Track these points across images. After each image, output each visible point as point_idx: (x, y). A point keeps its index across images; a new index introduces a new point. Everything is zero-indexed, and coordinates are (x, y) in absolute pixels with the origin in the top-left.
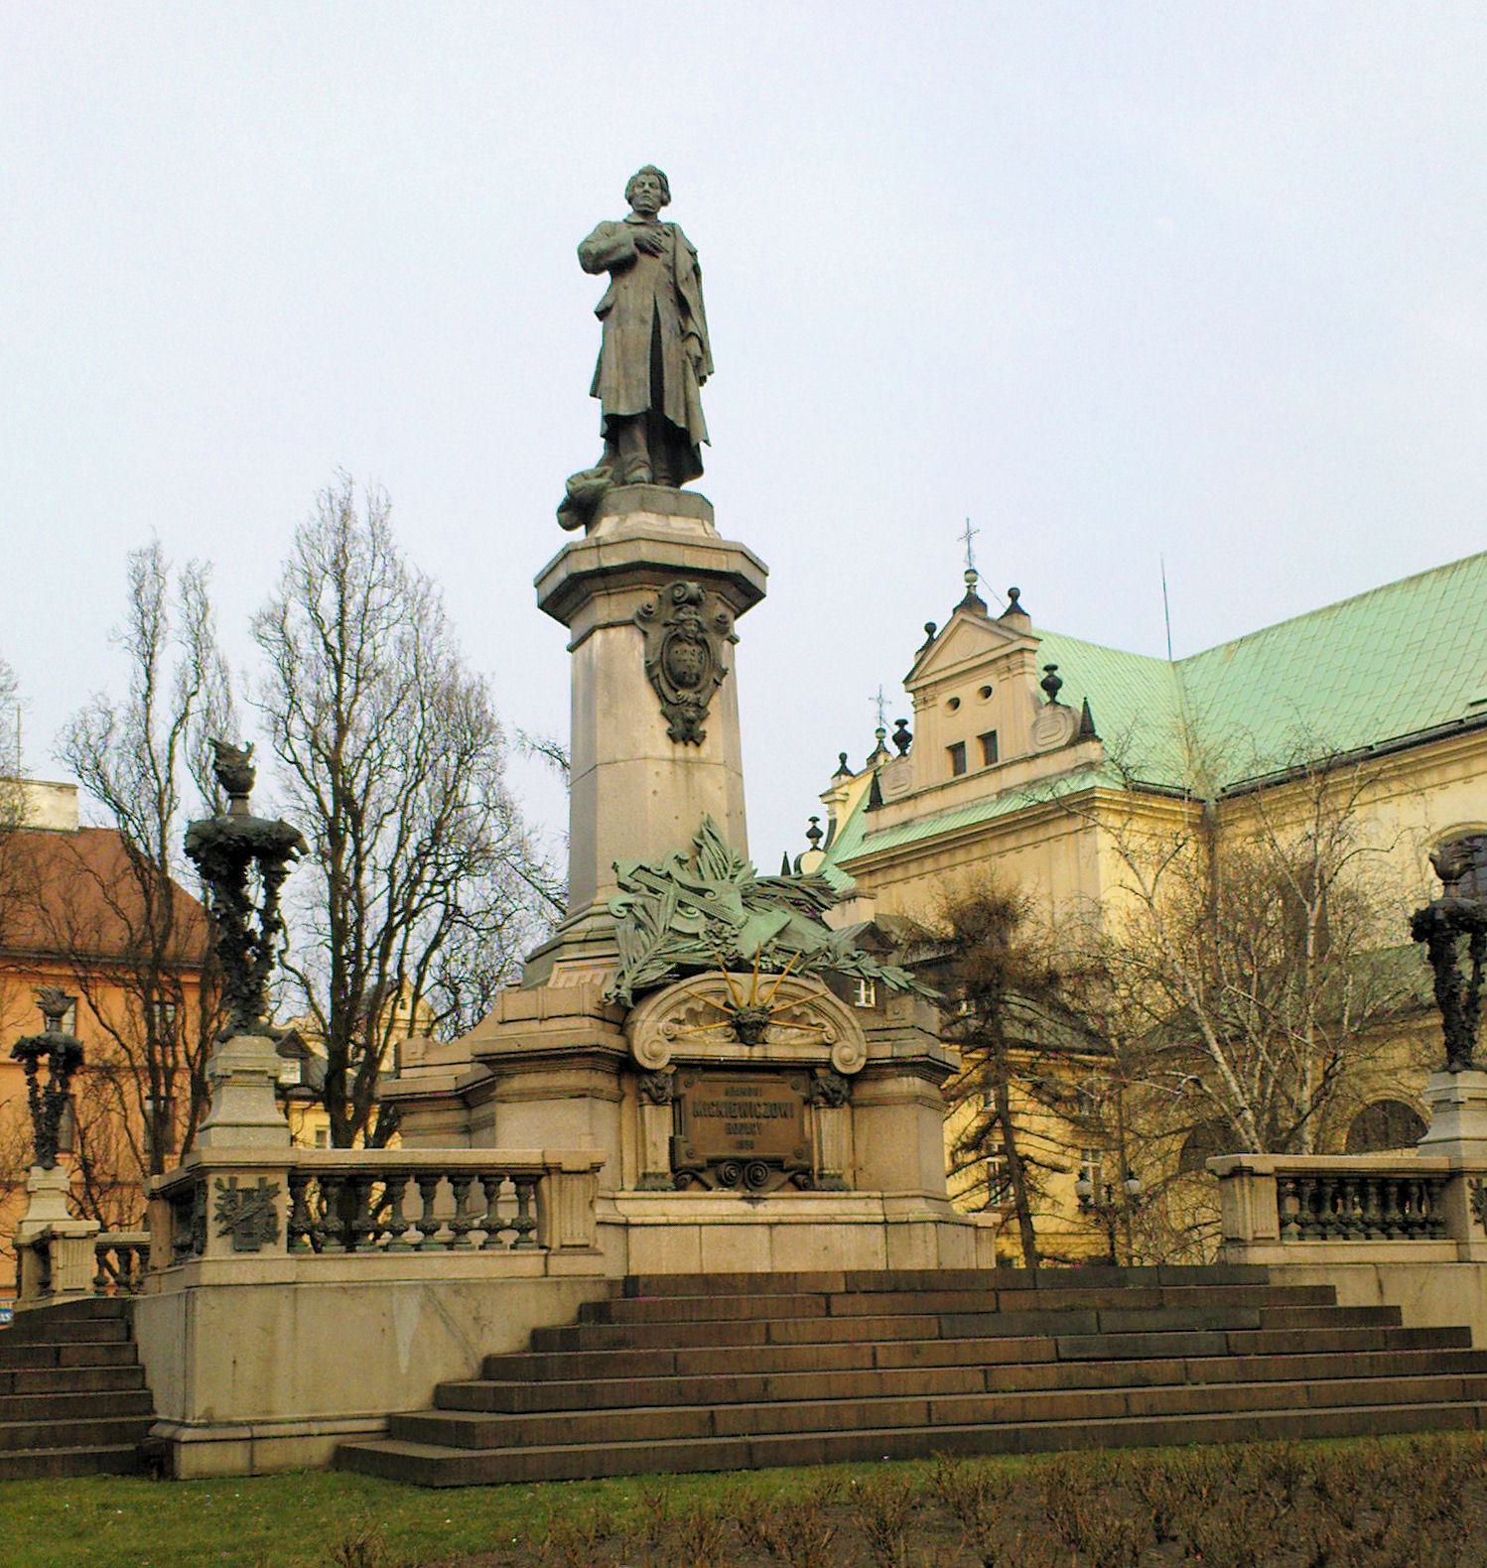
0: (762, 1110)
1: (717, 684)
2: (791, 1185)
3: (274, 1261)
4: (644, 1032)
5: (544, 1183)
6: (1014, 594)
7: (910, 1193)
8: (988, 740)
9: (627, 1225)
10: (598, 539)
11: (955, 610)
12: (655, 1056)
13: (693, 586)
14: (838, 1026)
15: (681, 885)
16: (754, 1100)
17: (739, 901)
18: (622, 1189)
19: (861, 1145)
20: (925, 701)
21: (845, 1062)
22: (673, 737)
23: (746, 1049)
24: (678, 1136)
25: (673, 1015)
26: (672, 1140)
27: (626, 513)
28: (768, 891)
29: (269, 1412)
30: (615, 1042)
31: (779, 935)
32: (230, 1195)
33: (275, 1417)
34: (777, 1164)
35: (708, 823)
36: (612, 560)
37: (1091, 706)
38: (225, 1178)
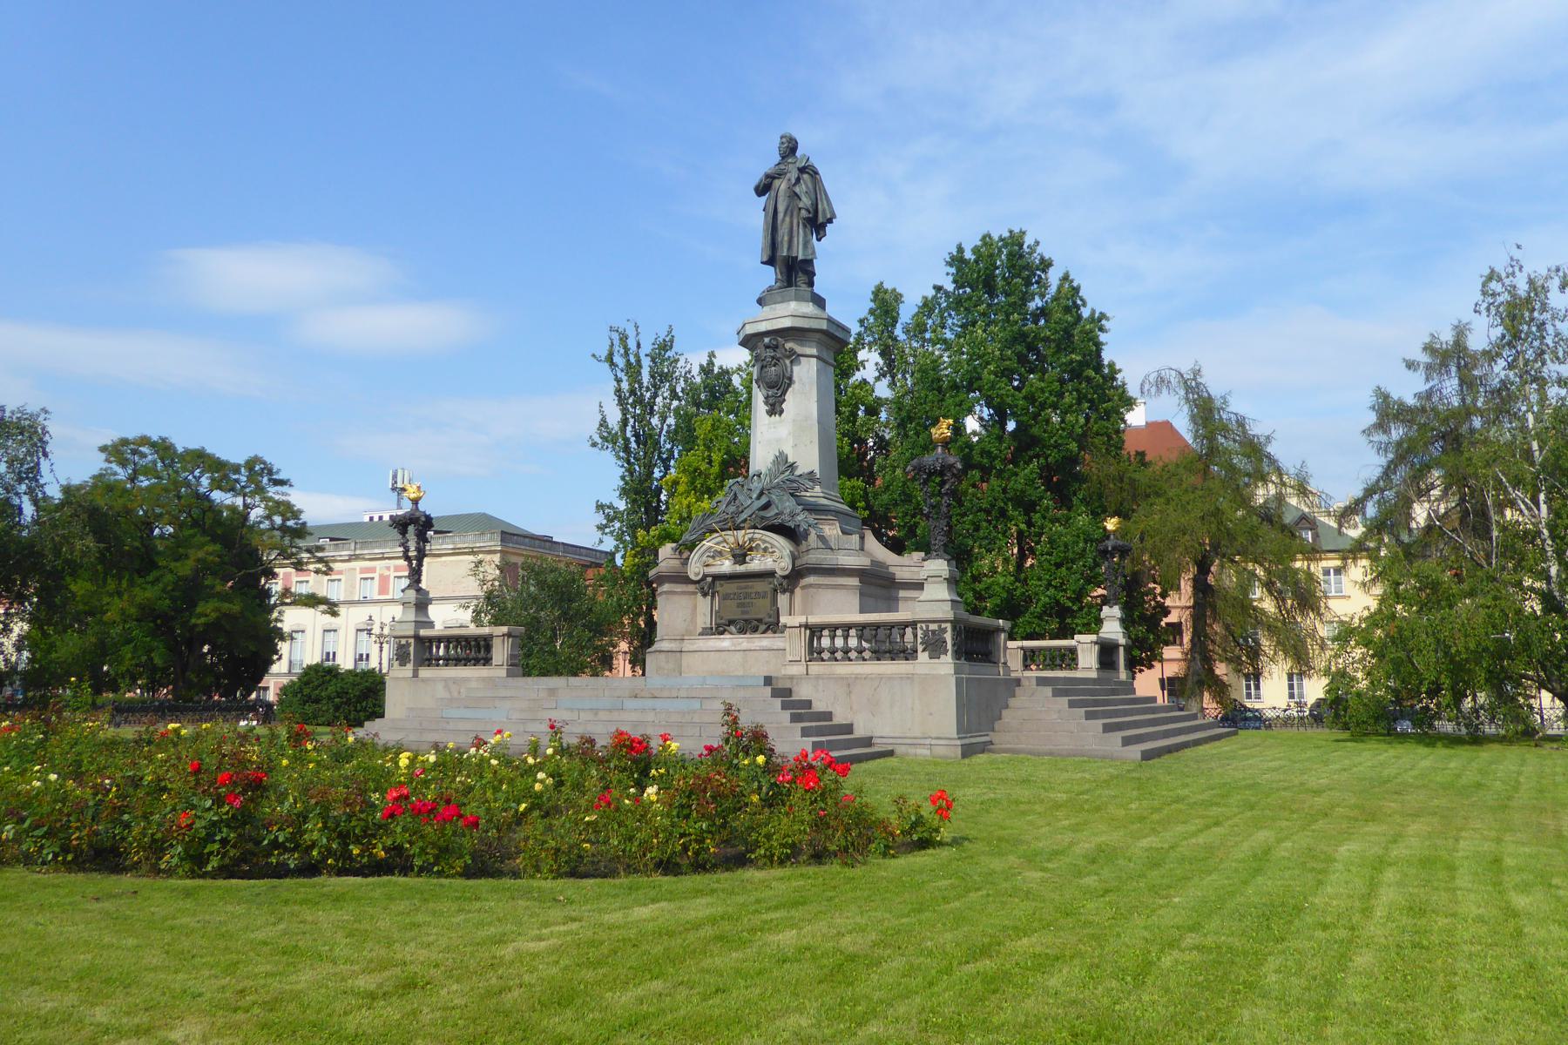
13: (767, 340)
34: (760, 621)
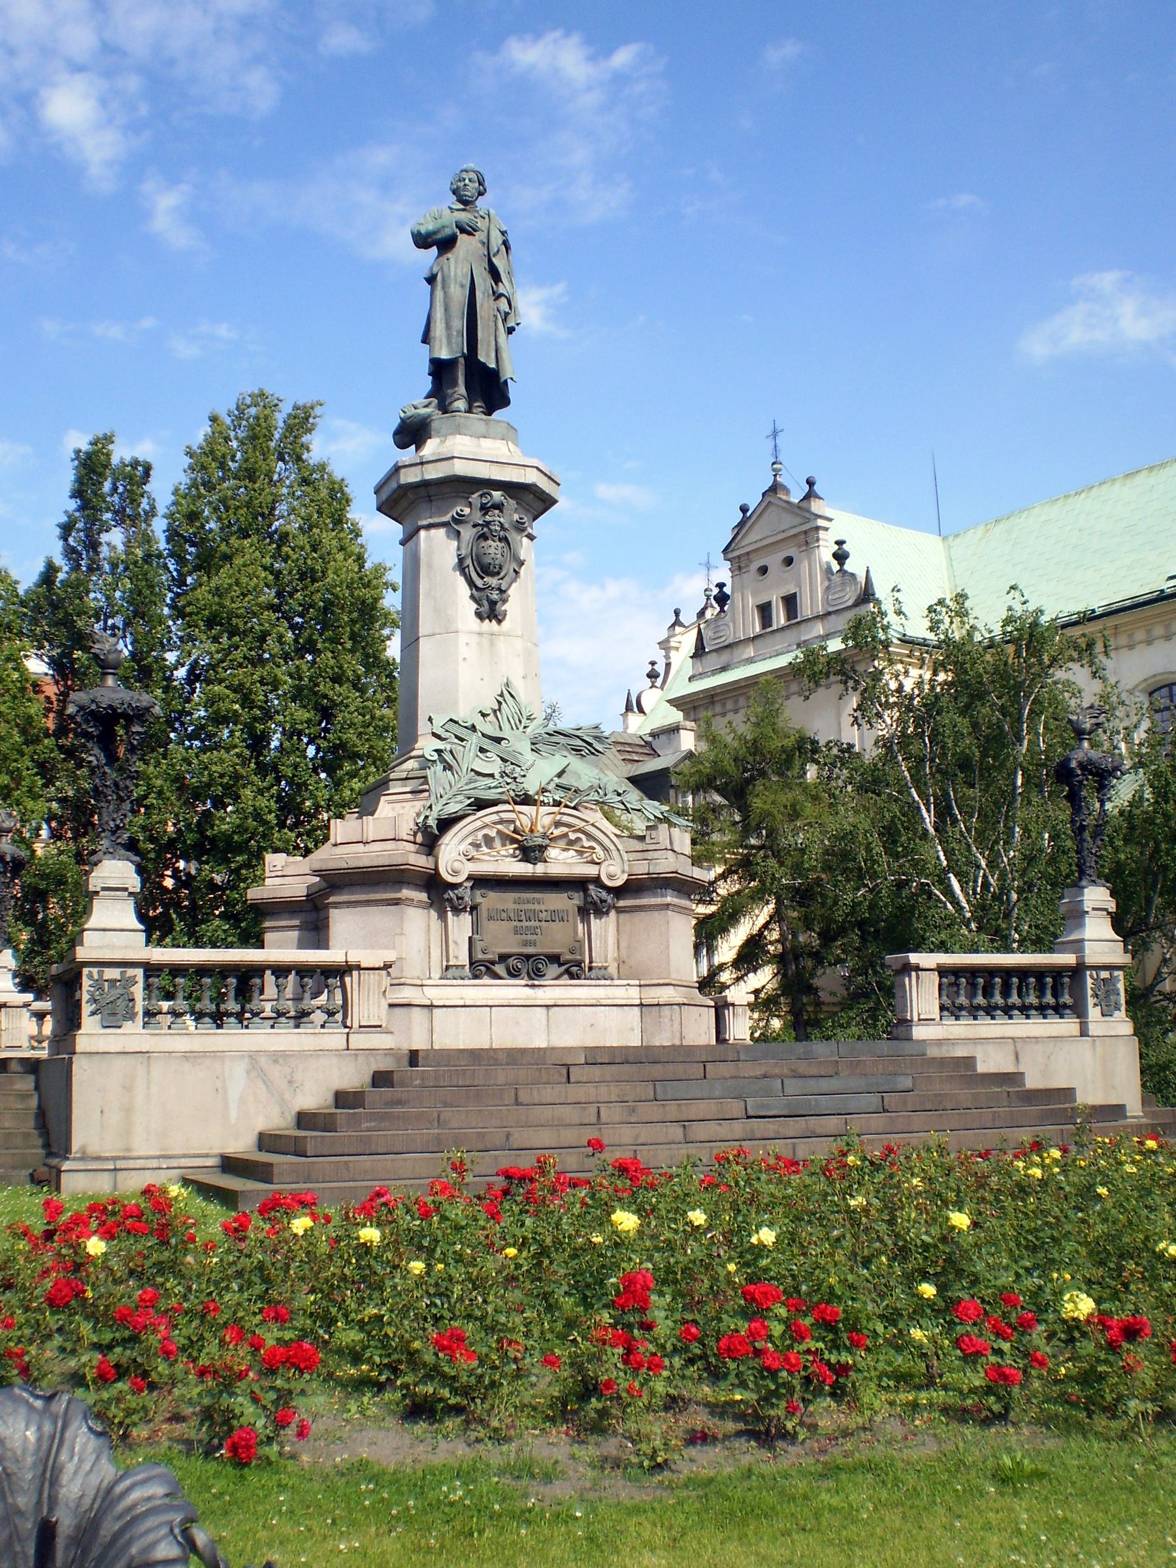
0: (543, 915)
2: (566, 976)
3: (133, 1034)
4: (447, 853)
5: (347, 979)
6: (810, 483)
7: (661, 981)
8: (790, 602)
9: (431, 1006)
10: (421, 457)
11: (764, 494)
12: (456, 873)
13: (497, 495)
14: (605, 849)
15: (483, 735)
16: (537, 907)
17: (529, 746)
18: (430, 978)
19: (623, 944)
20: (740, 568)
22: (479, 615)
23: (530, 866)
24: (475, 936)
26: (470, 938)
27: (445, 436)
28: (554, 739)
29: (128, 1150)
30: (422, 862)
31: (560, 775)
32: (98, 984)
33: (134, 1154)
34: (555, 959)
35: (507, 685)
36: (433, 473)
37: (872, 575)
38: (95, 971)
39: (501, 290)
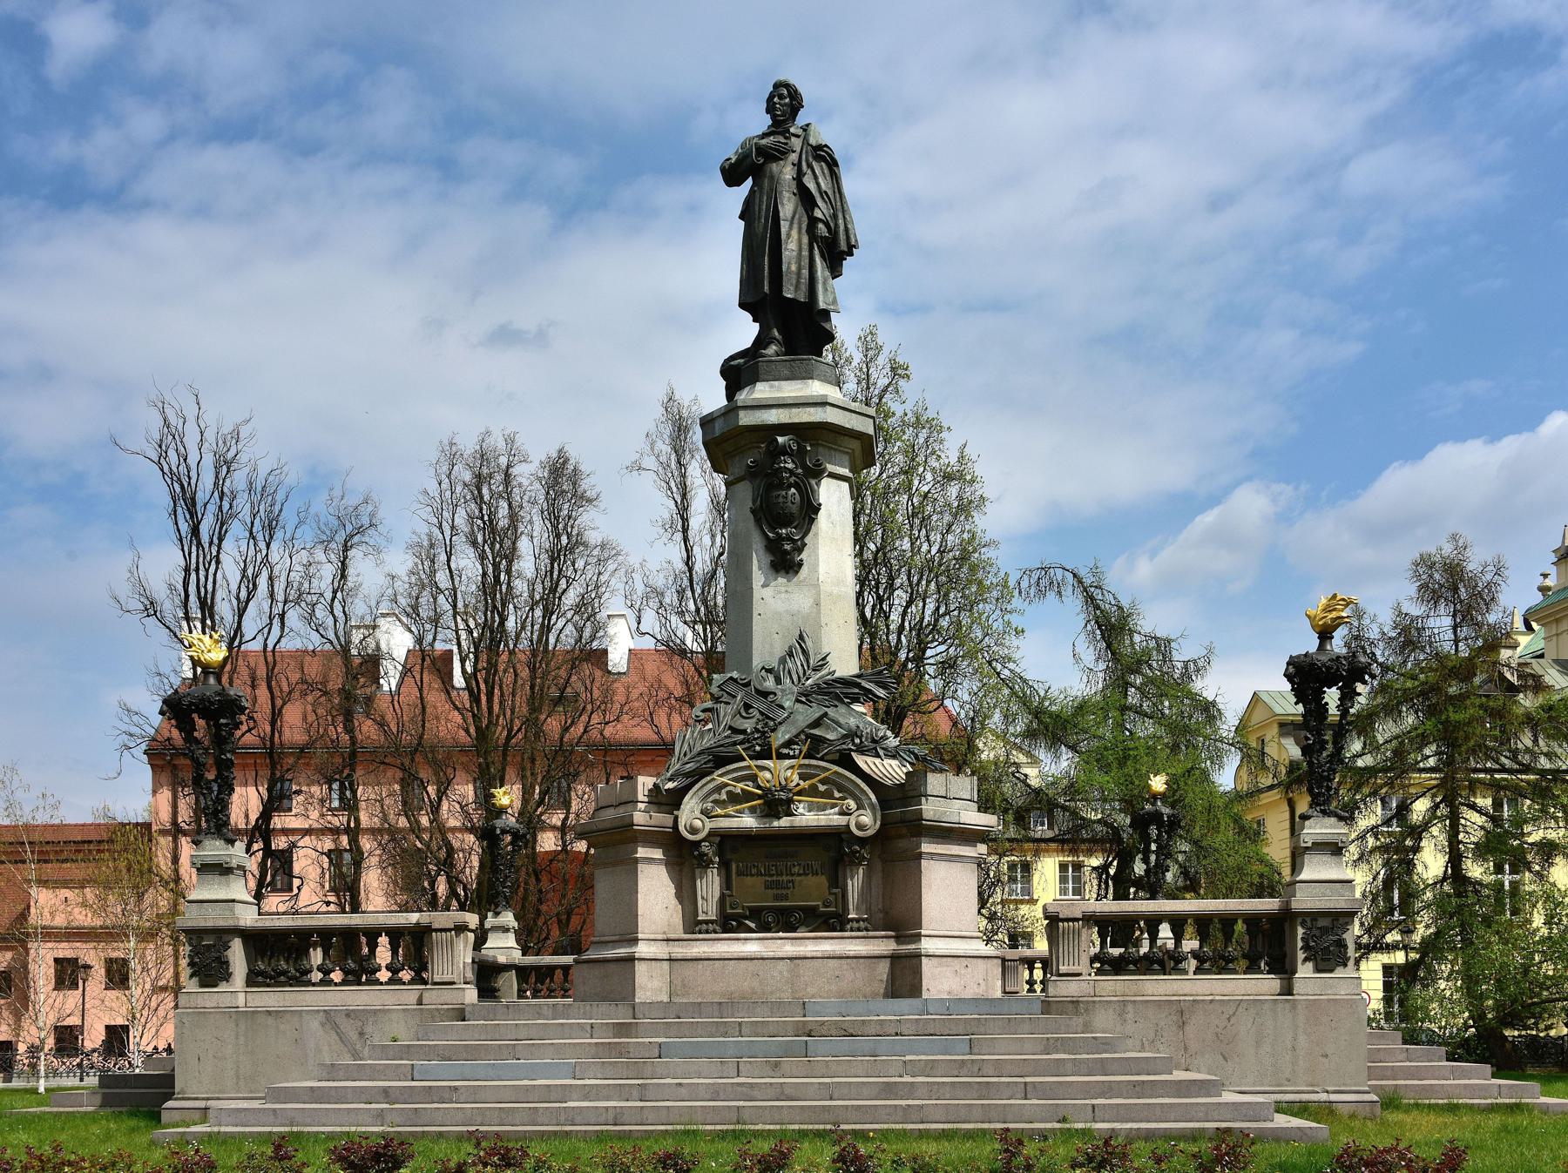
1: (812, 521)
12: (694, 831)
14: (855, 798)
21: (860, 827)
25: (716, 796)
31: (817, 723)
35: (801, 637)
39: (818, 214)
